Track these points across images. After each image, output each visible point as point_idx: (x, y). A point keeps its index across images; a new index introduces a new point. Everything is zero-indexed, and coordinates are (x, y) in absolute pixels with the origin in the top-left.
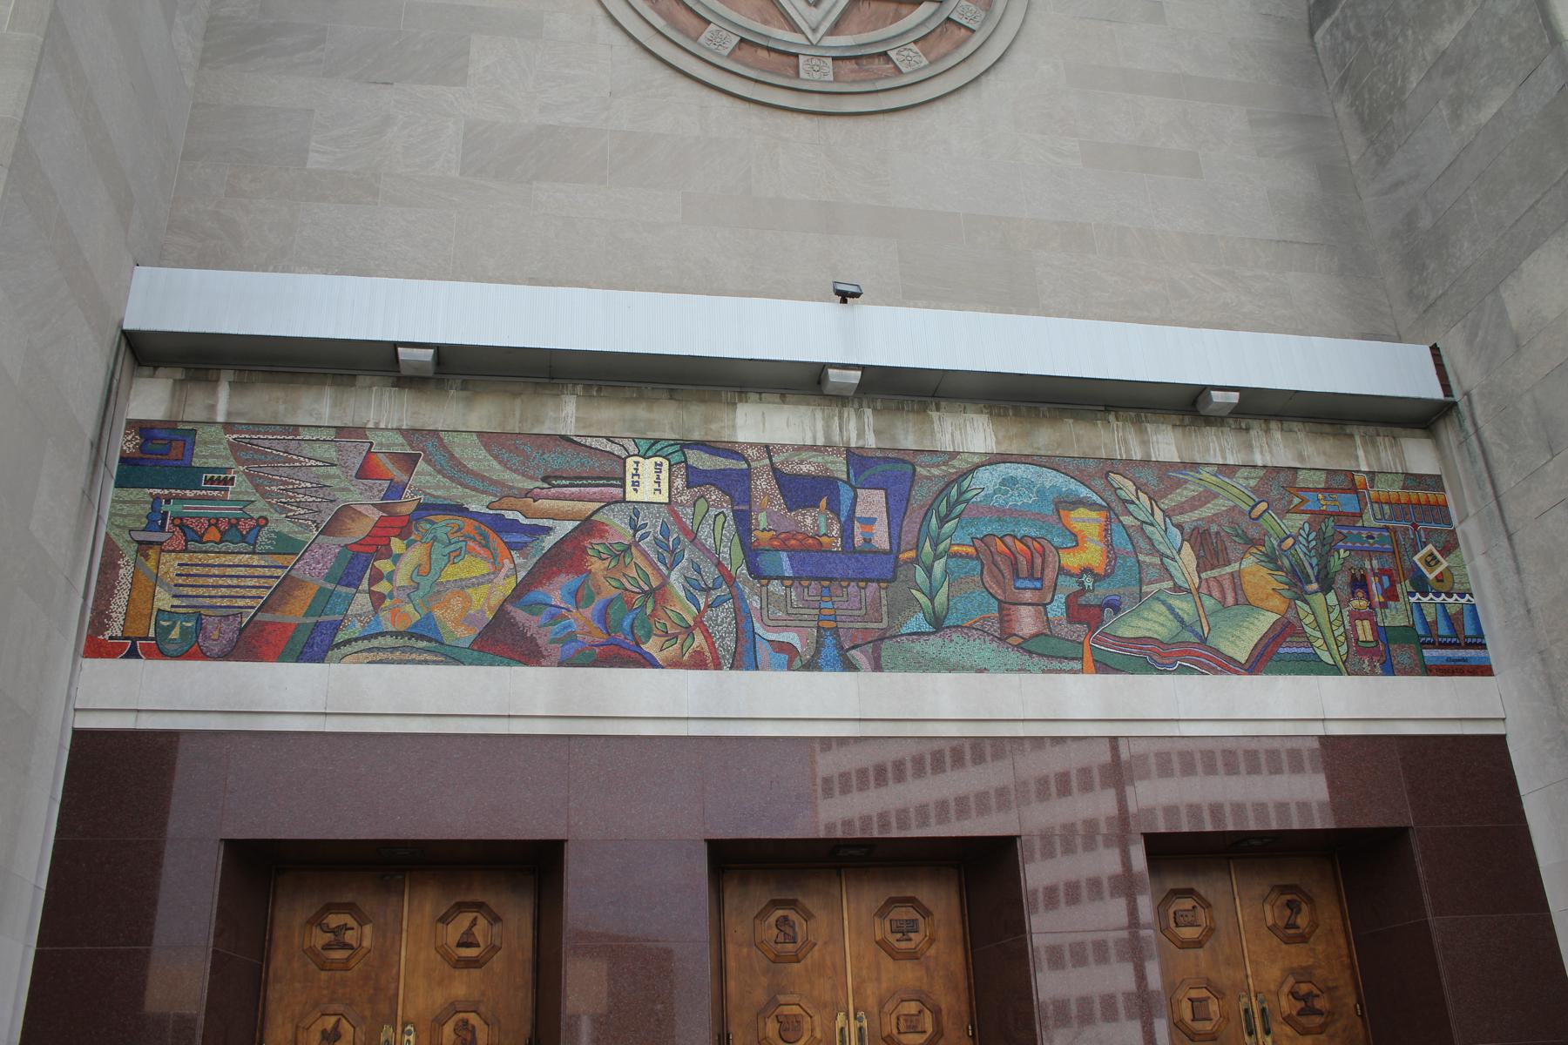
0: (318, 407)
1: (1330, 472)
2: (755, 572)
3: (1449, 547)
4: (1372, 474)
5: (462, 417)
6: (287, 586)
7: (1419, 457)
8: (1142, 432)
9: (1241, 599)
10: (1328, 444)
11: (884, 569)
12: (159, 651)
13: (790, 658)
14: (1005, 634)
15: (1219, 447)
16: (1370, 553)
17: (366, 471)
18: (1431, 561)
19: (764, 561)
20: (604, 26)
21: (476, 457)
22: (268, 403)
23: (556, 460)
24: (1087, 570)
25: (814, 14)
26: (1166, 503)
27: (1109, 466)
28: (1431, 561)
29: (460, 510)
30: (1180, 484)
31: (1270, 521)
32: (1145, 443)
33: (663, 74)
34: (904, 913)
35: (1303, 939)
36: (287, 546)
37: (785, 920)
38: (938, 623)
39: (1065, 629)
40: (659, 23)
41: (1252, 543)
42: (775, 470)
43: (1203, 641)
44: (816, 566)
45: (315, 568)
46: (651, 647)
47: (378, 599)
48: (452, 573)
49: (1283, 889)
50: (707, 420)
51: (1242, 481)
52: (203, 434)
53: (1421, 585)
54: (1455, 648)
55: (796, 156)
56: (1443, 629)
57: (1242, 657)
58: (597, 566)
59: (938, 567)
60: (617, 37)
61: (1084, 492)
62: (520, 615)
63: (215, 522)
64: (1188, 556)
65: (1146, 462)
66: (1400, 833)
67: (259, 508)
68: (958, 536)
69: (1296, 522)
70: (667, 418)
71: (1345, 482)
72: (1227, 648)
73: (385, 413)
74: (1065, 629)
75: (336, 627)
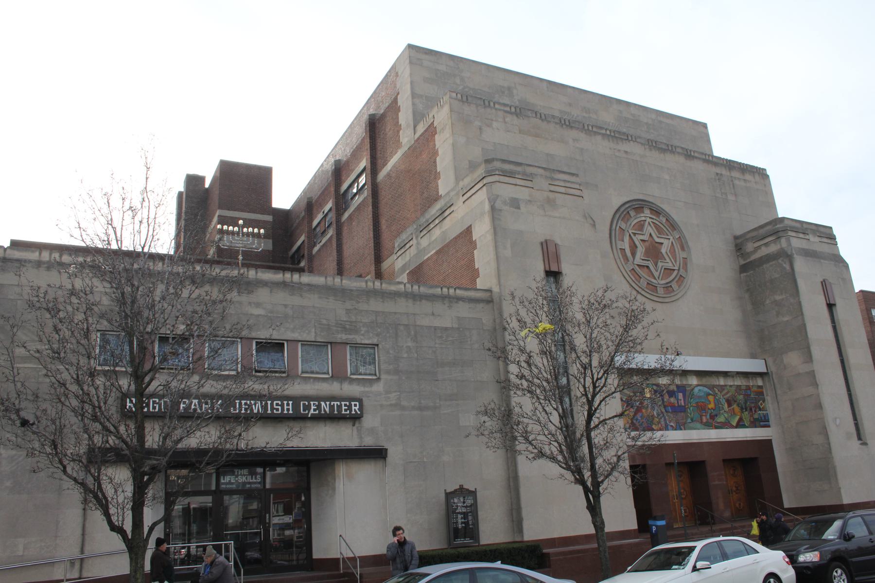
3: (764, 401)
7: (760, 382)
9: (734, 414)
11: (681, 409)
14: (702, 422)
15: (730, 382)
46: (654, 426)
51: (733, 389)
53: (760, 410)
54: (762, 422)
60: (625, 281)
64: (726, 405)
66: (755, 459)
68: (693, 402)
69: (741, 397)
71: (748, 388)
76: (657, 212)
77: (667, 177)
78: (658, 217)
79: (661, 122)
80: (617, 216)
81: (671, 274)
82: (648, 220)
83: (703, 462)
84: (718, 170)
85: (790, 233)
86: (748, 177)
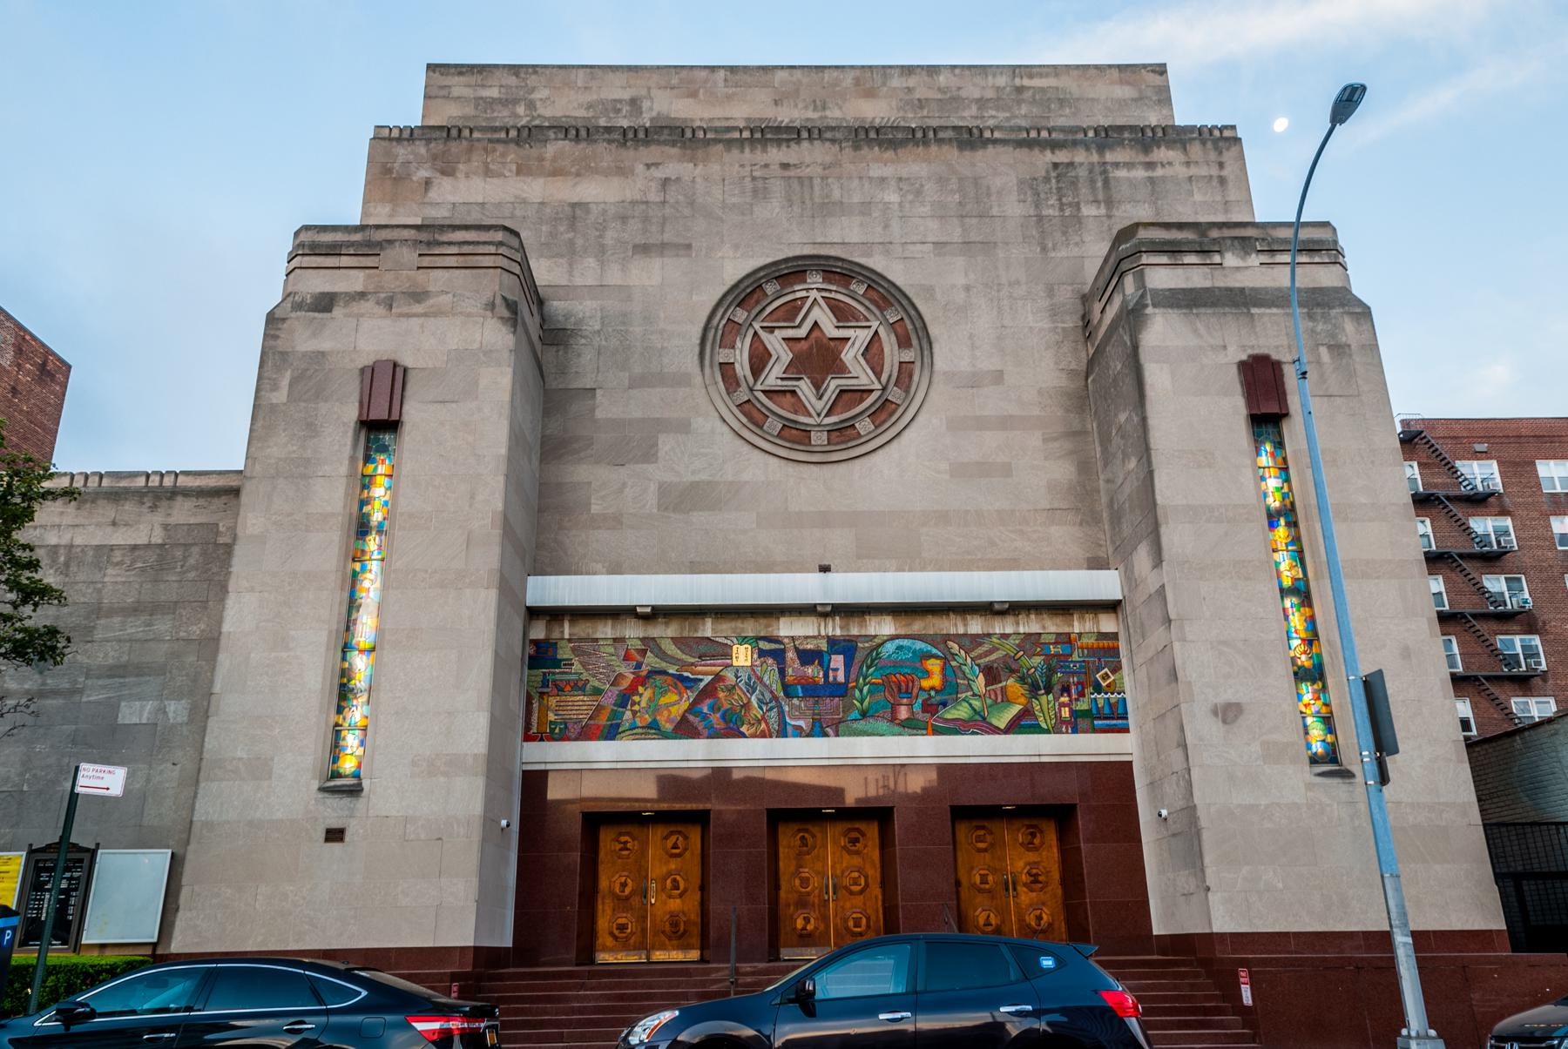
0: (606, 630)
1: (1058, 634)
2: (788, 695)
3: (1117, 669)
4: (1080, 634)
5: (665, 632)
6: (599, 709)
7: (1107, 624)
8: (965, 620)
9: (1007, 700)
10: (1058, 620)
11: (841, 691)
12: (551, 738)
13: (800, 732)
14: (893, 719)
15: (1004, 626)
16: (1073, 673)
17: (627, 657)
18: (1105, 677)
19: (791, 690)
20: (719, 423)
21: (671, 649)
22: (584, 629)
23: (702, 648)
24: (932, 688)
25: (819, 405)
26: (973, 654)
27: (947, 638)
28: (1105, 677)
29: (664, 673)
30: (981, 644)
31: (1025, 660)
32: (965, 625)
33: (747, 448)
34: (855, 835)
35: (1036, 849)
36: (597, 692)
37: (803, 838)
38: (864, 715)
39: (920, 716)
40: (744, 420)
41: (1012, 671)
42: (796, 648)
43: (984, 719)
44: (812, 691)
45: (609, 701)
46: (744, 729)
47: (634, 713)
48: (663, 701)
49: (1029, 827)
50: (767, 626)
51: (1013, 641)
52: (561, 644)
53: (1098, 688)
54: (1114, 719)
55: (807, 486)
56: (1106, 711)
57: (1002, 726)
58: (721, 695)
59: (866, 689)
60: (725, 429)
61: (934, 651)
62: (691, 718)
63: (568, 682)
64: (981, 679)
65: (965, 635)
67: (585, 676)
70: (750, 627)
71: (1066, 639)
72: (995, 722)
73: (633, 631)
74: (920, 716)
75: (618, 726)
76: (839, 271)
77: (893, 197)
78: (847, 286)
79: (1020, 90)
80: (730, 298)
81: (862, 401)
82: (814, 294)
83: (892, 809)
84: (1062, 156)
85: (1145, 259)
86: (1161, 154)
